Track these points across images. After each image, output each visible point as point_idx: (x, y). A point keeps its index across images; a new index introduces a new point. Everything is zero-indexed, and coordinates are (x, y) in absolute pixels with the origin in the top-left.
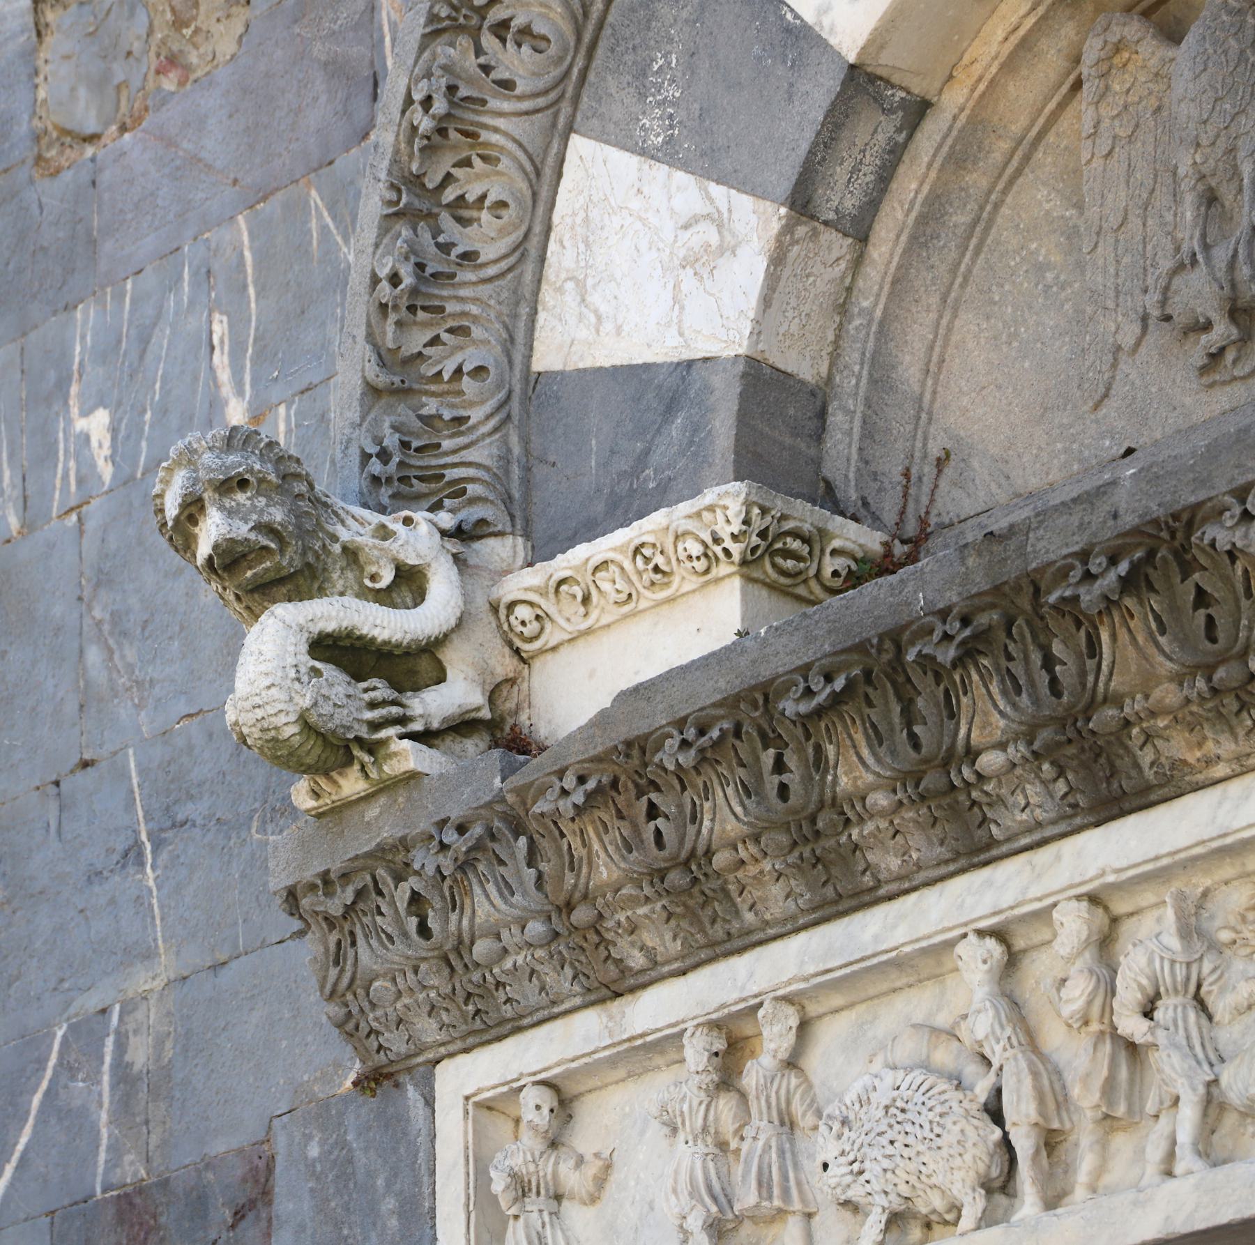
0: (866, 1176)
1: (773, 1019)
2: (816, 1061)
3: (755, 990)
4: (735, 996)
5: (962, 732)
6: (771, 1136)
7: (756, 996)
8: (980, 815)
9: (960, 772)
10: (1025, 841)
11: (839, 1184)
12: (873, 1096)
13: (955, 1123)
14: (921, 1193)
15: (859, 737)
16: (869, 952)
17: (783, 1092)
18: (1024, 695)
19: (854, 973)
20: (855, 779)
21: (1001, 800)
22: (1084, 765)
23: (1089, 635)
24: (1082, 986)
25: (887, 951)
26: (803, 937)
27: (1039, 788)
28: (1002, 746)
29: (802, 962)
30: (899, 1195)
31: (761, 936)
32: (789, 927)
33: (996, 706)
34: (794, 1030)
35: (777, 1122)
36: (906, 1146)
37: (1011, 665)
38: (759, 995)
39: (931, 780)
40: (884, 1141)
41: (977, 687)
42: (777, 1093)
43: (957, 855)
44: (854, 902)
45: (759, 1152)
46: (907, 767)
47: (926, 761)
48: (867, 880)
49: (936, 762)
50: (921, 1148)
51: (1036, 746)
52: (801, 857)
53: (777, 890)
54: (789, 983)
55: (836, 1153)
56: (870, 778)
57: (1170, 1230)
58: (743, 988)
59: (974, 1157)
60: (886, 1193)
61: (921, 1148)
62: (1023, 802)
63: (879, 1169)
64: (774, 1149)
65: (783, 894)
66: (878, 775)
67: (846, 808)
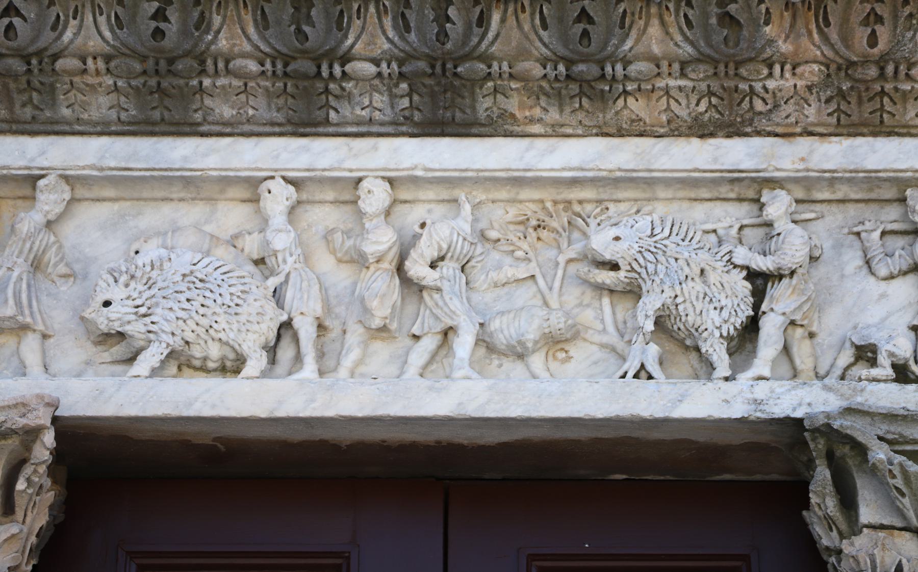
0: (154, 318)
1: (50, 189)
2: (69, 231)
3: (46, 164)
4: (22, 163)
5: (349, 42)
6: (24, 271)
7: (42, 169)
8: (324, 101)
9: (331, 67)
10: (354, 129)
11: (119, 319)
12: (166, 265)
13: (255, 300)
14: (202, 342)
15: (248, 18)
16: (177, 166)
17: (44, 243)
18: (413, 34)
19: (152, 177)
20: (234, 45)
21: (349, 97)
22: (433, 95)
23: (482, 12)
24: (390, 236)
25: (191, 170)
26: (105, 140)
27: (385, 98)
28: (376, 62)
29: (103, 157)
30: (182, 339)
31: (67, 128)
32: (99, 129)
33: (384, 32)
34: (65, 202)
35: (29, 263)
36: (202, 305)
37: (407, 12)
38: (47, 169)
39: (305, 65)
40: (182, 297)
41: (371, 17)
42: (41, 241)
43: (289, 122)
44: (172, 129)
45: (14, 279)
46: (284, 50)
47: (304, 52)
48: (198, 117)
49: (311, 55)
50: (218, 310)
51: (404, 69)
52: (144, 85)
53: (105, 101)
54: (84, 168)
55: (124, 296)
56: (248, 48)
57: (463, 412)
58: (33, 160)
59: (269, 327)
60: (173, 334)
61: (218, 310)
62: (367, 103)
63: (174, 317)
64: (25, 281)
65: (108, 105)
66: (257, 48)
67: (209, 62)
